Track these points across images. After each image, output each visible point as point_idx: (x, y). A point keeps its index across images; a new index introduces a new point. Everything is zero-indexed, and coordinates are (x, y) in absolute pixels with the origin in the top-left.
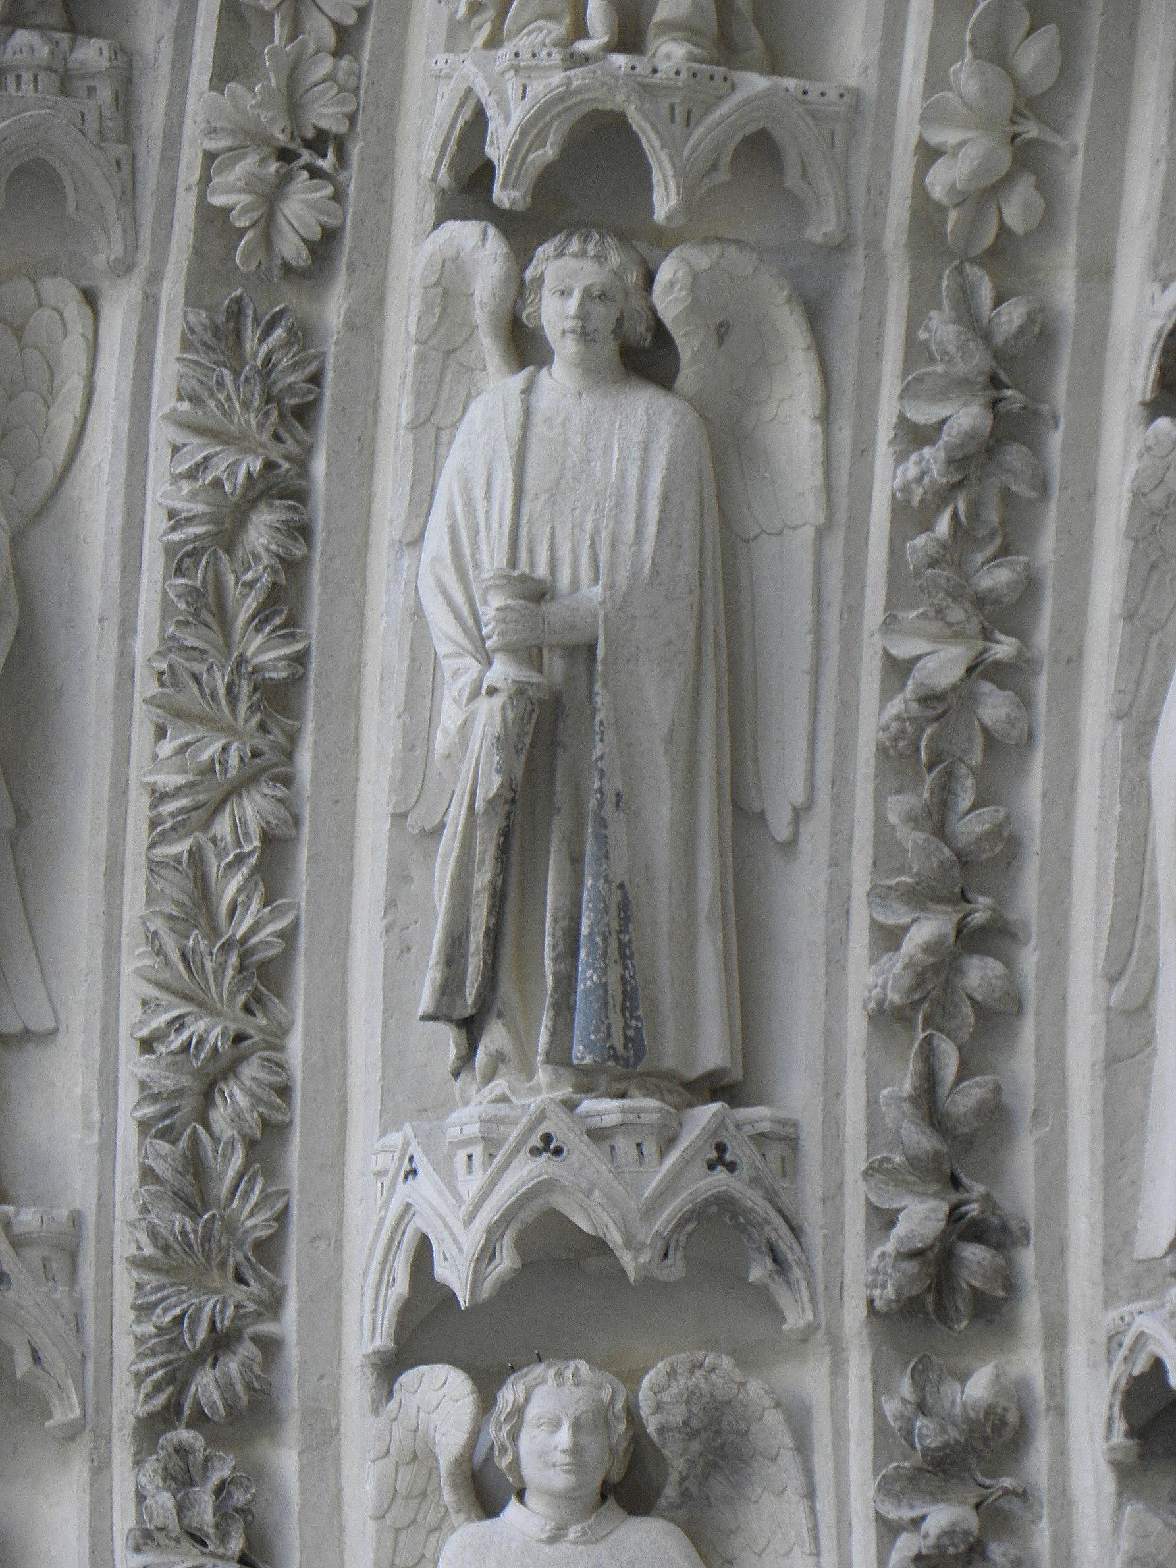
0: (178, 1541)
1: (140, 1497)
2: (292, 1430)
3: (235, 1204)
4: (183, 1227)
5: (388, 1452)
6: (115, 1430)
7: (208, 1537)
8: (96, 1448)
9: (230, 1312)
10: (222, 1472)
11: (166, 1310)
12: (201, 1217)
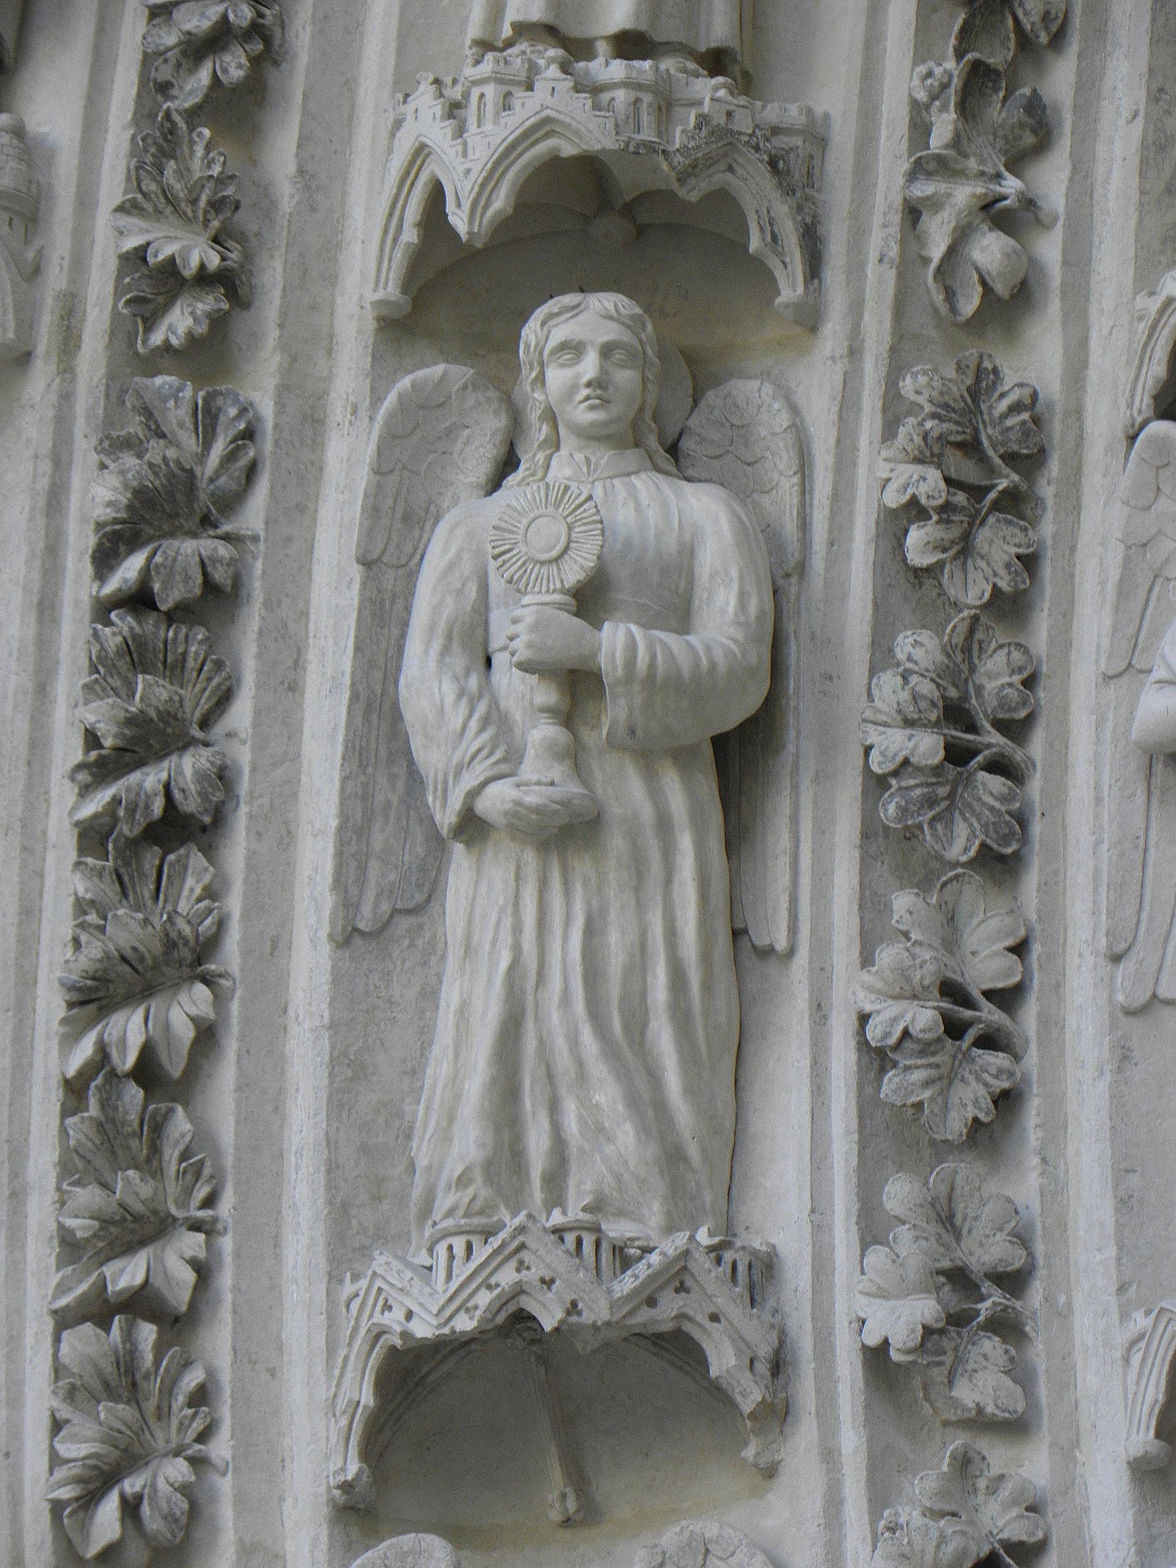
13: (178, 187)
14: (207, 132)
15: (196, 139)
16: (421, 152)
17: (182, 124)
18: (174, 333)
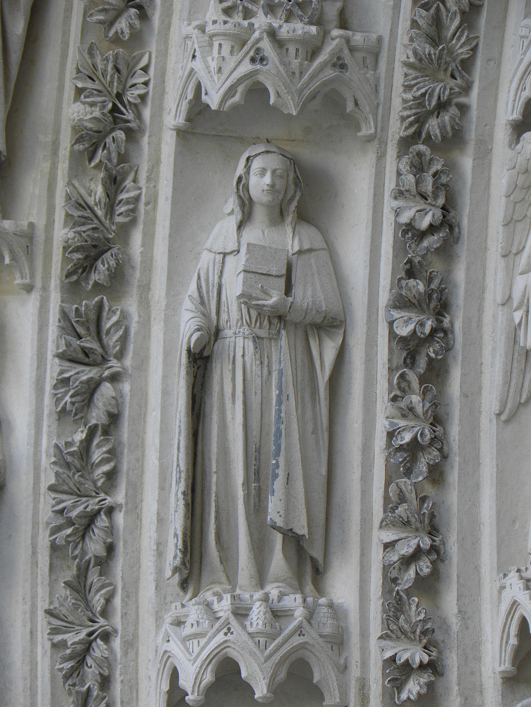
0: (415, 196)
1: (399, 174)
2: (471, 148)
3: (454, 42)
4: (430, 52)
5: (514, 167)
6: (389, 140)
7: (429, 196)
8: (380, 147)
9: (447, 92)
10: (437, 166)
11: (418, 89)
12: (439, 47)
13: (406, 627)
14: (416, 599)
15: (412, 602)
16: (515, 604)
17: (404, 596)
18: (411, 694)
